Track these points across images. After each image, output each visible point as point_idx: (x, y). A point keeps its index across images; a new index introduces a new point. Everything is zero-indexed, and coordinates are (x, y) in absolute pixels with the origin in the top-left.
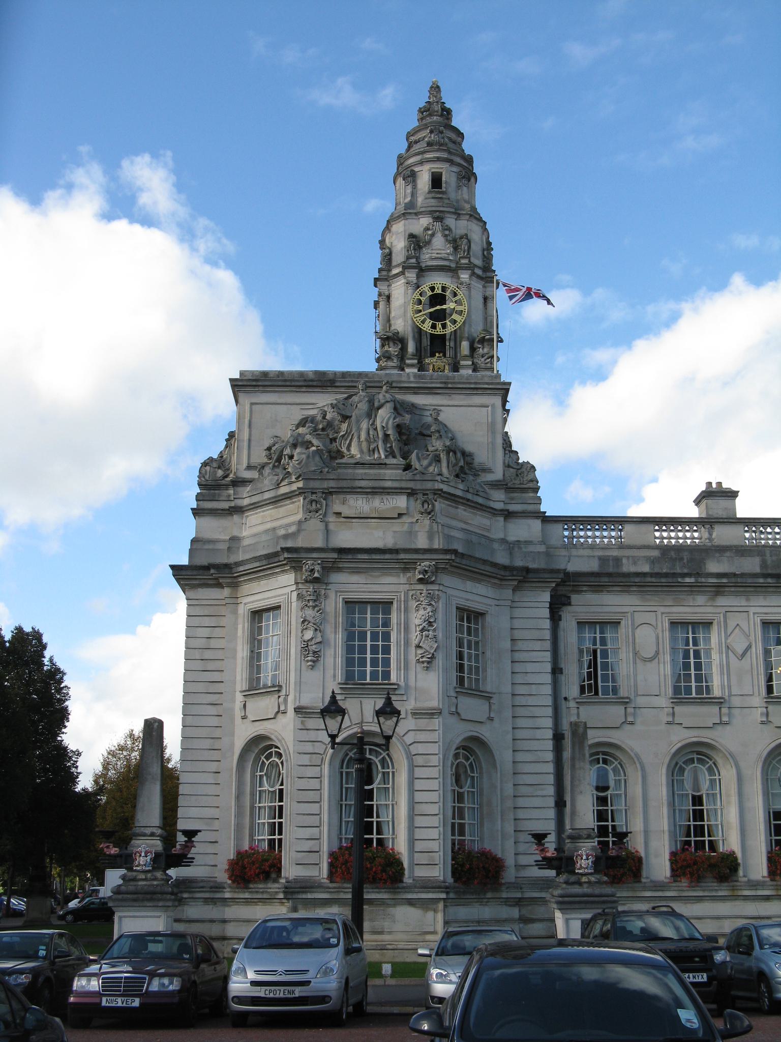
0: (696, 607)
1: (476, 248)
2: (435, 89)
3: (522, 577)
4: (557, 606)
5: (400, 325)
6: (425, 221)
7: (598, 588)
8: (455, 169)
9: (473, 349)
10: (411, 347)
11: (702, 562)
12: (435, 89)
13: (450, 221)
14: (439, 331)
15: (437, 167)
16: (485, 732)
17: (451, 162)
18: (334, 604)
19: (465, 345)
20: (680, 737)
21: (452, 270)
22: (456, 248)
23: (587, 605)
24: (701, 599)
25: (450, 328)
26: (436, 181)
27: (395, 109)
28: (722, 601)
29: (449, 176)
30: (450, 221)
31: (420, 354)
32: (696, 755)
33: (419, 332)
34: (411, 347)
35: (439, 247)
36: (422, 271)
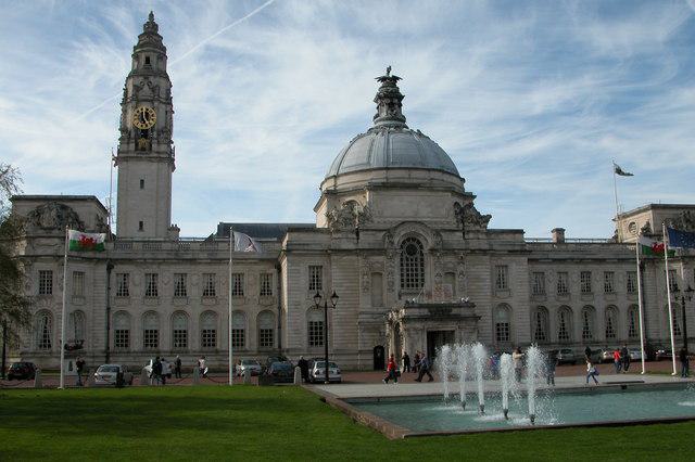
0: (154, 269)
1: (163, 90)
2: (151, 15)
4: (109, 269)
5: (129, 126)
6: (141, 79)
7: (122, 264)
9: (159, 135)
10: (133, 135)
12: (151, 15)
13: (151, 79)
16: (83, 308)
17: (154, 52)
19: (155, 133)
20: (146, 308)
23: (119, 268)
24: (154, 266)
25: (149, 127)
26: (148, 60)
28: (162, 267)
29: (153, 59)
30: (151, 79)
33: (136, 129)
34: (133, 135)
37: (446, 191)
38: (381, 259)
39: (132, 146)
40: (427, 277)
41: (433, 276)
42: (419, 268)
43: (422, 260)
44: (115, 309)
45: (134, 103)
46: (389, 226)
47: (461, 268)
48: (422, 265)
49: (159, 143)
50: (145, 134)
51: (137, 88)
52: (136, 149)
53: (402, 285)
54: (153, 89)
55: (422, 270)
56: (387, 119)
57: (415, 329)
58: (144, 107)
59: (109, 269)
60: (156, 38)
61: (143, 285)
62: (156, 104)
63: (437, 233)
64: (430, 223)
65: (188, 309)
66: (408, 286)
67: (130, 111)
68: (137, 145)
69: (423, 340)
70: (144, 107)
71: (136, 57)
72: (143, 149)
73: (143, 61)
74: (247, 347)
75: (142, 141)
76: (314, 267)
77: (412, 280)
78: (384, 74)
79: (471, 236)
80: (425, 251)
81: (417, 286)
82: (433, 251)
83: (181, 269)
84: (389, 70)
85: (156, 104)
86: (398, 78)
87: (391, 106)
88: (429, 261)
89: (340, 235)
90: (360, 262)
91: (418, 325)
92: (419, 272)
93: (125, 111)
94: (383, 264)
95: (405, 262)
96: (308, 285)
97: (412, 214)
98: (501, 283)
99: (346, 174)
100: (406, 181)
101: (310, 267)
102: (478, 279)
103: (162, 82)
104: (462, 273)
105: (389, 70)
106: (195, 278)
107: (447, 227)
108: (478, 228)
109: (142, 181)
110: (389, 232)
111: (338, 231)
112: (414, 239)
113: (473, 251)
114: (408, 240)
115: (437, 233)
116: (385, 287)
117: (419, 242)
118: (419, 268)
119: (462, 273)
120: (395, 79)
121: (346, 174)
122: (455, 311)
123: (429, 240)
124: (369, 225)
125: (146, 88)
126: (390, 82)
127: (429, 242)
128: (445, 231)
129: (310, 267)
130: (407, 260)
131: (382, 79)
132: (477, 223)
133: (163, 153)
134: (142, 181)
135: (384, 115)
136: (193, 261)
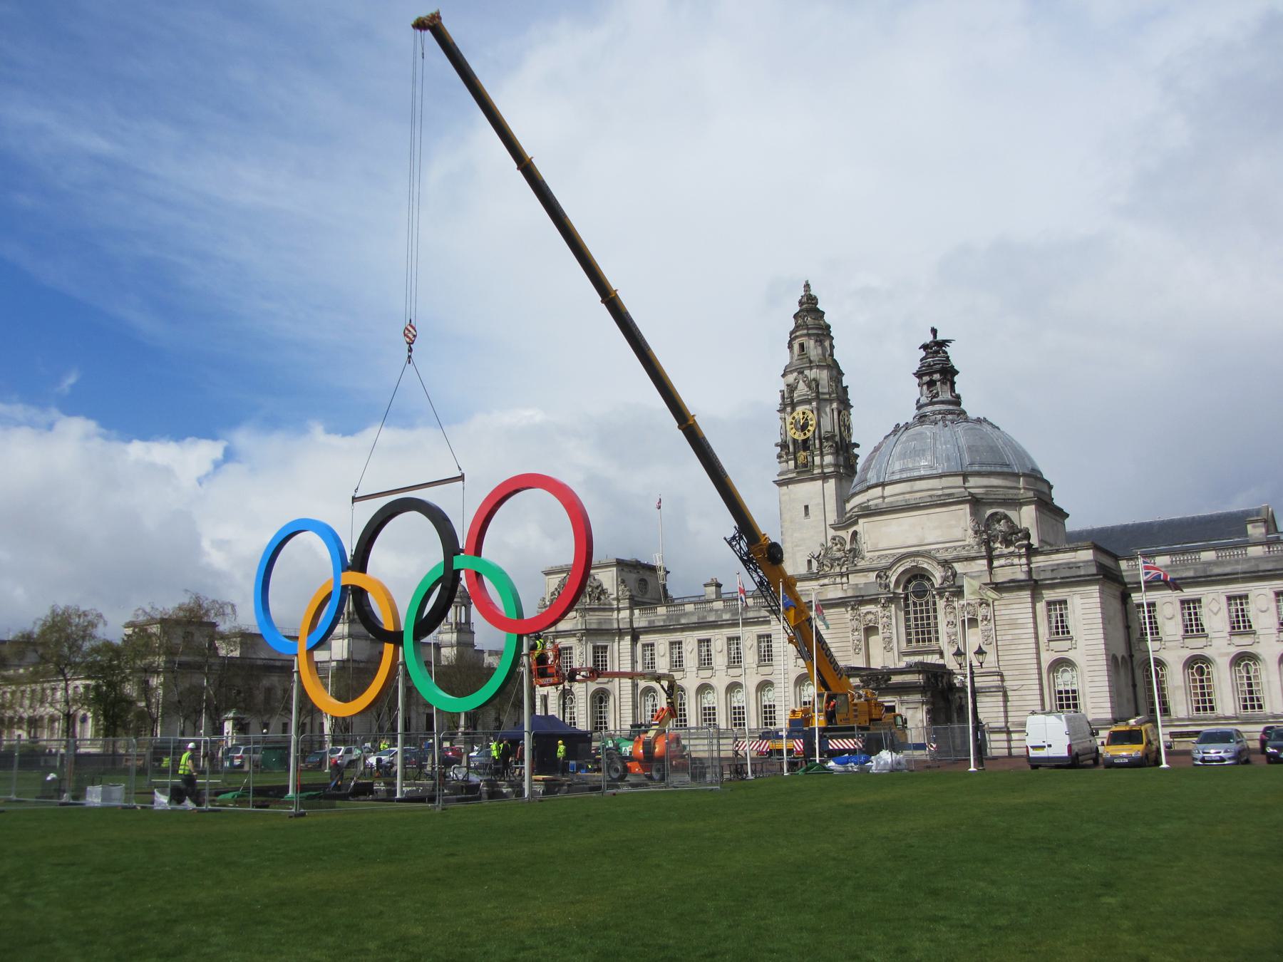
0: (676, 637)
2: (807, 286)
3: (620, 633)
4: (635, 639)
9: (821, 443)
11: (678, 620)
12: (807, 286)
13: (807, 372)
14: (803, 437)
23: (644, 639)
26: (802, 346)
31: (795, 453)
36: (794, 406)
39: (792, 463)
40: (940, 628)
43: (935, 604)
45: (789, 409)
46: (884, 563)
49: (822, 455)
50: (805, 445)
52: (796, 467)
53: (909, 641)
55: (936, 618)
59: (635, 639)
61: (668, 655)
63: (946, 564)
64: (938, 550)
65: (713, 682)
66: (918, 641)
68: (796, 459)
71: (790, 346)
72: (805, 465)
73: (796, 347)
74: (1219, 711)
75: (802, 455)
78: (929, 338)
79: (1002, 562)
81: (930, 640)
83: (703, 634)
84: (934, 331)
86: (949, 341)
88: (941, 604)
89: (826, 581)
92: (932, 621)
95: (911, 608)
97: (915, 542)
98: (1061, 630)
100: (907, 496)
102: (1013, 624)
105: (934, 331)
107: (964, 553)
109: (806, 507)
110: (882, 573)
111: (825, 576)
115: (946, 564)
118: (931, 614)
120: (943, 344)
122: (896, 679)
124: (862, 564)
125: (801, 385)
126: (936, 347)
128: (958, 559)
130: (915, 604)
131: (925, 347)
134: (806, 507)
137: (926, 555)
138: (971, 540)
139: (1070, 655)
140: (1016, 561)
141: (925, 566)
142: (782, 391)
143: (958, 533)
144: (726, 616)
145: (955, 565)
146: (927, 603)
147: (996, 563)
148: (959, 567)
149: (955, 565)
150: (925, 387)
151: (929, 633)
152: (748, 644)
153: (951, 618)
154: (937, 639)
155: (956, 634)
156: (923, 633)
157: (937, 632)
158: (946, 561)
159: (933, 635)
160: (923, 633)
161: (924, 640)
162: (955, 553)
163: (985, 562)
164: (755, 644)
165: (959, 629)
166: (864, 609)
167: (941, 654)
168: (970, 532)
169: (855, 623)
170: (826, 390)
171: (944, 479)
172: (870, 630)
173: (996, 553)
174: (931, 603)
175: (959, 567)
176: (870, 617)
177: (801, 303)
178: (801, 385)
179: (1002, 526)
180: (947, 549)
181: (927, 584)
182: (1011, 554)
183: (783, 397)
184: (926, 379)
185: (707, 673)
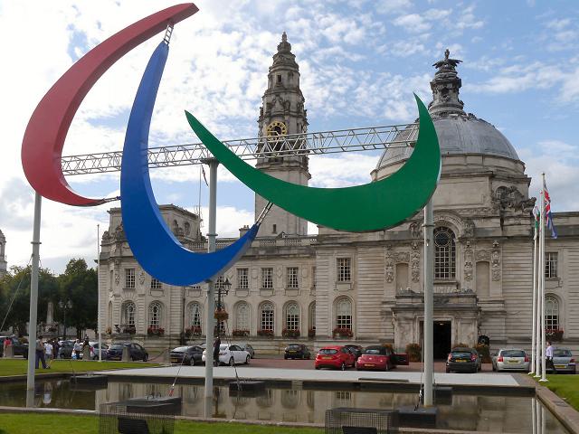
1: (293, 104)
6: (273, 97)
8: (287, 72)
12: (284, 36)
13: (283, 96)
15: (279, 73)
16: (162, 299)
18: (122, 270)
21: (282, 116)
22: (284, 107)
26: (279, 77)
27: (271, 42)
29: (285, 76)
32: (291, 303)
35: (278, 106)
36: (271, 117)
37: (482, 176)
38: (406, 249)
40: (457, 267)
41: (463, 267)
42: (450, 257)
43: (454, 249)
44: (189, 300)
45: (267, 120)
47: (495, 256)
48: (454, 254)
51: (270, 105)
54: (283, 104)
55: (454, 260)
56: (441, 106)
57: (406, 319)
58: (276, 122)
60: (289, 57)
62: (286, 118)
63: (469, 220)
64: (462, 210)
65: (249, 300)
67: (265, 126)
69: (414, 330)
70: (276, 122)
71: (270, 77)
73: (275, 79)
76: (342, 259)
77: (443, 270)
79: (512, 221)
80: (456, 240)
81: (447, 276)
82: (463, 240)
84: (447, 53)
85: (286, 118)
86: (457, 61)
87: (444, 92)
88: (460, 249)
90: (384, 253)
91: (410, 315)
92: (450, 261)
93: (261, 127)
94: (408, 255)
96: (336, 276)
97: (443, 204)
99: (384, 167)
101: (338, 259)
103: (294, 98)
104: (496, 262)
106: (255, 272)
107: (482, 213)
108: (520, 212)
112: (445, 228)
113: (511, 239)
114: (439, 229)
115: (469, 220)
116: (411, 277)
117: (451, 231)
118: (450, 257)
119: (496, 262)
120: (454, 63)
121: (384, 167)
122: (453, 302)
123: (460, 228)
125: (277, 105)
127: (459, 229)
128: (477, 217)
129: (338, 259)
131: (439, 65)
132: (519, 207)
133: (293, 162)
135: (436, 103)
136: (253, 258)
137: (451, 212)
138: (488, 204)
139: (557, 292)
140: (523, 222)
141: (451, 221)
142: (262, 109)
143: (478, 198)
144: (262, 253)
145: (475, 221)
146: (447, 249)
147: (505, 223)
148: (478, 224)
149: (475, 221)
150: (439, 93)
151: (447, 270)
152: (279, 273)
153: (468, 260)
154: (454, 275)
155: (471, 272)
156: (442, 270)
157: (454, 270)
158: (468, 219)
159: (450, 272)
160: (442, 270)
161: (442, 276)
162: (475, 213)
163: (499, 221)
164: (285, 273)
165: (474, 269)
166: (399, 249)
167: (458, 285)
168: (489, 198)
169: (389, 261)
170: (294, 110)
171: (458, 158)
172: (402, 265)
173: (508, 214)
174: (450, 249)
175: (478, 224)
176: (403, 256)
177: (279, 47)
178: (277, 105)
179: (512, 196)
180: (468, 210)
181: (449, 236)
182: (519, 216)
183: (262, 112)
184: (441, 87)
185: (242, 294)
